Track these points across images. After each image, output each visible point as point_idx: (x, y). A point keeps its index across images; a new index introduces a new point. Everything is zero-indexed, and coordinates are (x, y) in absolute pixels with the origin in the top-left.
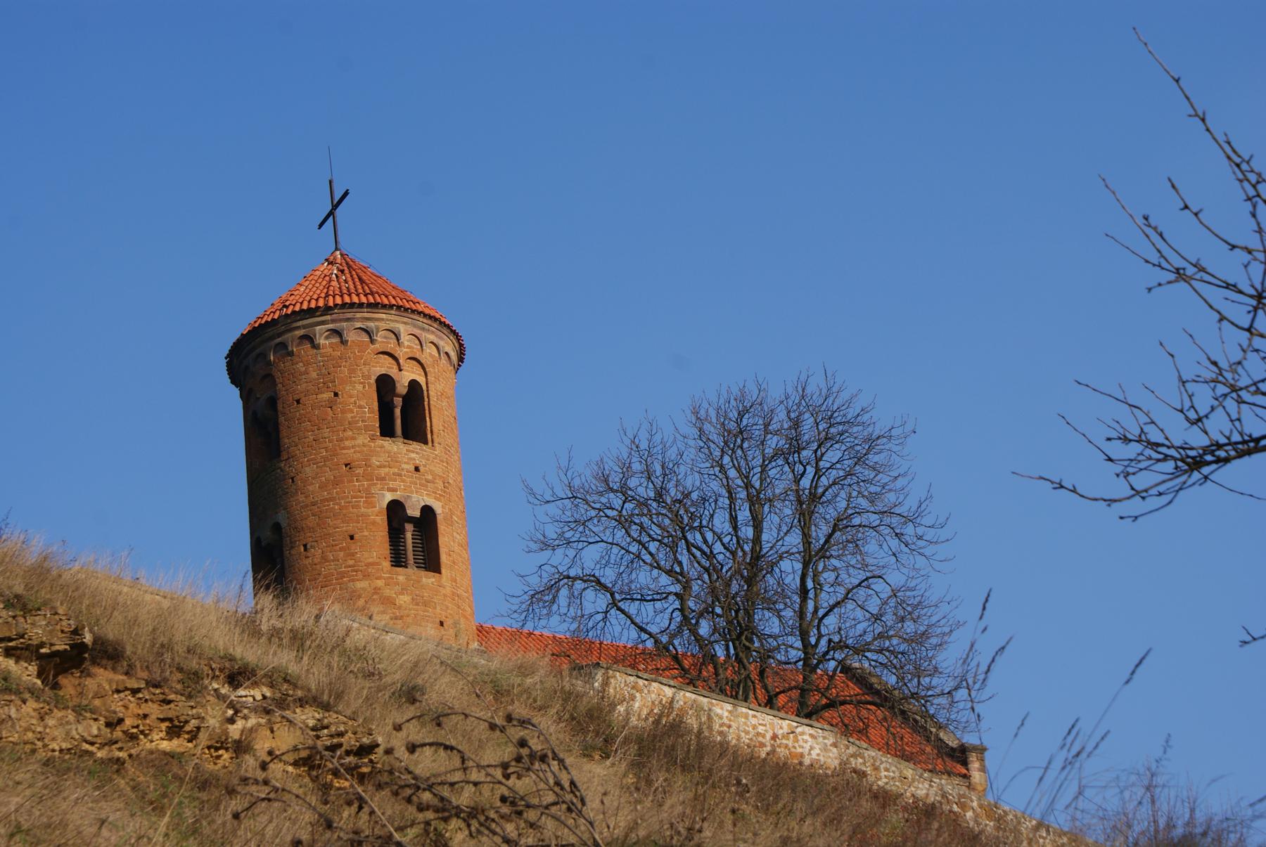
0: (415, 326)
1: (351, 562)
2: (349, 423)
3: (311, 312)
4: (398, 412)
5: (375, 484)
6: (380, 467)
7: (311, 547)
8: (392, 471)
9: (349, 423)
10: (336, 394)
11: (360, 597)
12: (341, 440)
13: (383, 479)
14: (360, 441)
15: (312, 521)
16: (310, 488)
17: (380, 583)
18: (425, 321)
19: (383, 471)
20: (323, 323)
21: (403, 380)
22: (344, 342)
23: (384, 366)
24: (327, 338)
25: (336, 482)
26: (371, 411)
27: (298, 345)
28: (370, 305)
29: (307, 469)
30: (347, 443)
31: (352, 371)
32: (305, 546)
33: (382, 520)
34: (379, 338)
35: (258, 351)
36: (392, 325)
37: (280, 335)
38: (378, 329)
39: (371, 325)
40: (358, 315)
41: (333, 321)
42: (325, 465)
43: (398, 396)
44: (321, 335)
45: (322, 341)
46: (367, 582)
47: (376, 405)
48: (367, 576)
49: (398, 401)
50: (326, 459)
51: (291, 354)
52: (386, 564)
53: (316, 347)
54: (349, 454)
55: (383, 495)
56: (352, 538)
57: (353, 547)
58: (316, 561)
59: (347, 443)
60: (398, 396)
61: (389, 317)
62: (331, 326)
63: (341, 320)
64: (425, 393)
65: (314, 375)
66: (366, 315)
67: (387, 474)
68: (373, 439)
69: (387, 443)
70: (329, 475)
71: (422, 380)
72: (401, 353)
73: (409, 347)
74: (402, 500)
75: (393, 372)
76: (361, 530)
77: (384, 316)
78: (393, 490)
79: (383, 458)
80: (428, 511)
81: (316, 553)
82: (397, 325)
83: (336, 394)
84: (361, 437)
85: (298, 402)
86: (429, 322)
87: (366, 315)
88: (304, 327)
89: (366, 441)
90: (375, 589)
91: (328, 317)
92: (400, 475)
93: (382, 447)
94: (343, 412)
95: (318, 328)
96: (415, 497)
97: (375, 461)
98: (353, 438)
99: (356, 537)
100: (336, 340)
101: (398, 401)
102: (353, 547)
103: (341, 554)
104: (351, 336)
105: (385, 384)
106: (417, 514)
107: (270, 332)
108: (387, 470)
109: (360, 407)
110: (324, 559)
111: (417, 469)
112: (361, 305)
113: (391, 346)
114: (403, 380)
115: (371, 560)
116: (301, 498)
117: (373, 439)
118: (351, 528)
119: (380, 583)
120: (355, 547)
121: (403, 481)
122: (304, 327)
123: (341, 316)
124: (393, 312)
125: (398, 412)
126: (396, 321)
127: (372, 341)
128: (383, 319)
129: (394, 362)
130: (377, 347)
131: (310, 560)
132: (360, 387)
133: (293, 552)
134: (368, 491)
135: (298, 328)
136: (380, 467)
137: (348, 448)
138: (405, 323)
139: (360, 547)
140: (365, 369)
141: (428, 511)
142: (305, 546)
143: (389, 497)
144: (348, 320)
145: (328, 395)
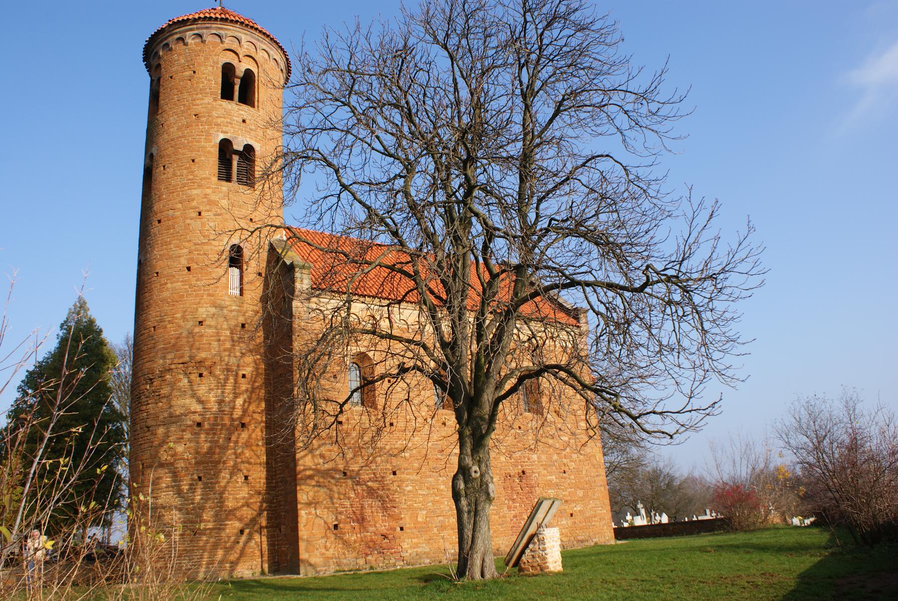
0: (252, 37)
1: (191, 177)
2: (201, 90)
3: (184, 22)
4: (237, 88)
5: (213, 128)
6: (217, 117)
7: (168, 167)
8: (226, 120)
9: (201, 90)
10: (194, 72)
11: (193, 200)
12: (194, 100)
13: (219, 125)
14: (206, 100)
15: (170, 151)
16: (171, 130)
17: (209, 191)
18: (260, 35)
19: (219, 120)
20: (191, 30)
21: (241, 69)
22: (203, 42)
23: (230, 58)
24: (193, 39)
25: (188, 126)
26: (216, 83)
27: (176, 44)
28: (222, 19)
29: (171, 118)
30: (198, 102)
31: (206, 59)
32: (164, 166)
33: (215, 151)
34: (227, 41)
36: (236, 34)
37: (166, 39)
38: (226, 35)
39: (222, 32)
40: (214, 26)
41: (198, 28)
42: (182, 116)
43: (238, 78)
44: (189, 37)
45: (189, 41)
46: (200, 190)
47: (220, 80)
48: (200, 186)
49: (238, 82)
50: (183, 112)
51: (171, 50)
52: (215, 179)
53: (186, 44)
54: (199, 109)
55: (218, 135)
56: (193, 161)
57: (193, 167)
58: (169, 176)
59: (198, 102)
60: (238, 78)
61: (235, 29)
62: (196, 32)
63: (202, 28)
64: (256, 78)
65: (182, 61)
66: (219, 26)
67: (222, 122)
68: (215, 100)
69: (225, 103)
70: (184, 122)
71: (255, 70)
72: (241, 53)
73: (247, 49)
74: (231, 139)
75: (235, 62)
76: (200, 156)
77: (231, 28)
79: (221, 112)
80: (249, 149)
81: (170, 171)
82: (240, 34)
83: (194, 72)
84: (208, 98)
85: (171, 77)
86: (263, 37)
87: (219, 26)
88: (180, 32)
89: (210, 101)
90: (205, 195)
91: (195, 26)
92: (231, 124)
93: (221, 105)
94: (198, 83)
95: (188, 33)
96: (240, 138)
97: (214, 114)
98: (203, 99)
99: (196, 160)
100: (198, 40)
101: (238, 82)
102: (193, 167)
103: (185, 172)
104: (209, 39)
105: (228, 70)
106: (241, 149)
107: (161, 37)
108: (223, 119)
109: (209, 80)
110: (175, 175)
111: (244, 121)
112: (216, 19)
113: (235, 46)
114: (241, 69)
115: (204, 176)
116: (166, 136)
117: (215, 100)
118: (193, 155)
119: (209, 191)
120: (194, 167)
121: (233, 127)
122: (180, 32)
123: (203, 26)
125: (237, 88)
127: (222, 42)
129: (236, 56)
130: (226, 46)
131: (166, 176)
132: (210, 68)
133: (157, 171)
135: (176, 33)
136: (217, 117)
137: (198, 105)
138: (245, 34)
139: (198, 167)
140: (215, 58)
141: (249, 149)
142: (164, 166)
143: (222, 136)
144: (207, 28)
145: (189, 73)
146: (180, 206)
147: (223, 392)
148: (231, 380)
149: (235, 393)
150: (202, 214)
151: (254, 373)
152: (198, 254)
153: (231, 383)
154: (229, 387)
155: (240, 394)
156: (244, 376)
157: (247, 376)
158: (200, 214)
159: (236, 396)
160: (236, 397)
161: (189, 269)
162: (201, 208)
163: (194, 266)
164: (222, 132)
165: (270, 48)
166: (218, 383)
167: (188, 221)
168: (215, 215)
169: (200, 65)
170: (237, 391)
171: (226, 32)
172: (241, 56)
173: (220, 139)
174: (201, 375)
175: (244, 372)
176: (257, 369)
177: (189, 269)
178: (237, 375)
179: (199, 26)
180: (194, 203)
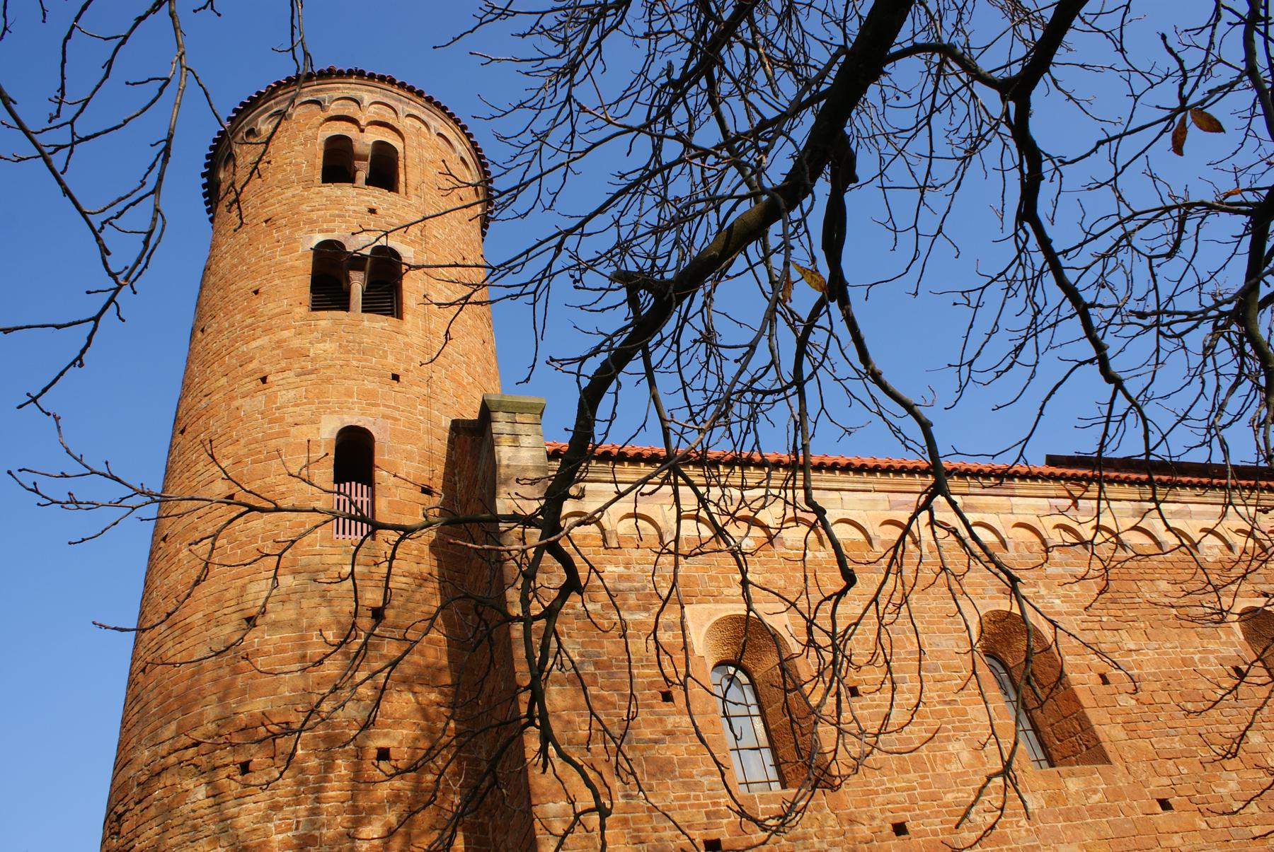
18: (401, 92)
19: (314, 216)
26: (313, 165)
36: (352, 94)
39: (321, 96)
41: (276, 104)
43: (364, 158)
52: (303, 310)
54: (275, 208)
60: (364, 158)
64: (401, 155)
86: (409, 95)
88: (248, 124)
95: (260, 119)
109: (297, 164)
113: (351, 110)
120: (258, 302)
122: (248, 124)
124: (351, 81)
126: (360, 90)
128: (338, 88)
130: (331, 113)
138: (366, 91)
143: (319, 238)
147: (314, 812)
148: (342, 767)
149: (355, 810)
150: (270, 379)
151: (424, 744)
152: (254, 462)
153: (340, 778)
154: (335, 791)
155: (372, 810)
156: (384, 754)
157: (393, 753)
158: (264, 380)
159: (359, 817)
160: (357, 823)
164: (321, 231)
165: (429, 116)
166: (301, 783)
168: (298, 375)
170: (363, 803)
171: (331, 94)
172: (363, 123)
173: (314, 244)
174: (245, 768)
175: (382, 743)
176: (430, 732)
178: (360, 754)
179: (278, 99)
180: (254, 365)
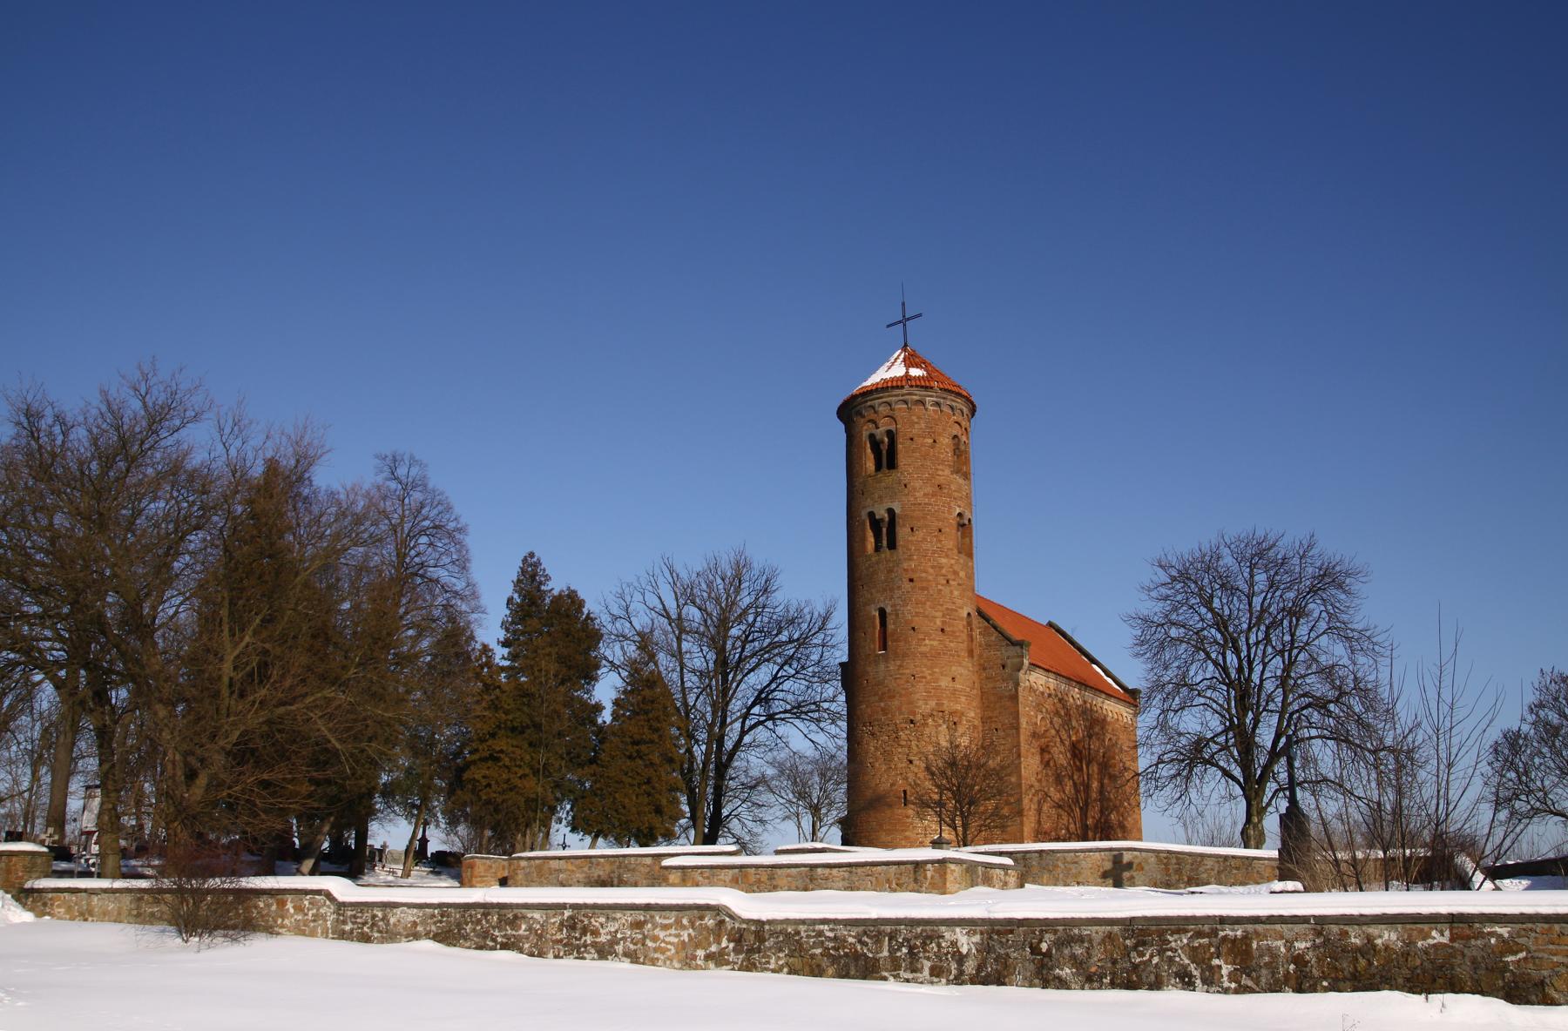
1: (939, 545)
23: (956, 430)
30: (940, 473)
35: (884, 400)
39: (954, 404)
48: (947, 556)
62: (934, 399)
75: (959, 435)
78: (959, 506)
83: (935, 441)
134: (949, 504)
143: (958, 511)
146: (931, 571)
158: (948, 581)
161: (942, 630)
162: (949, 577)
163: (947, 629)
167: (940, 587)
169: (940, 435)
177: (942, 630)
180: (944, 571)
